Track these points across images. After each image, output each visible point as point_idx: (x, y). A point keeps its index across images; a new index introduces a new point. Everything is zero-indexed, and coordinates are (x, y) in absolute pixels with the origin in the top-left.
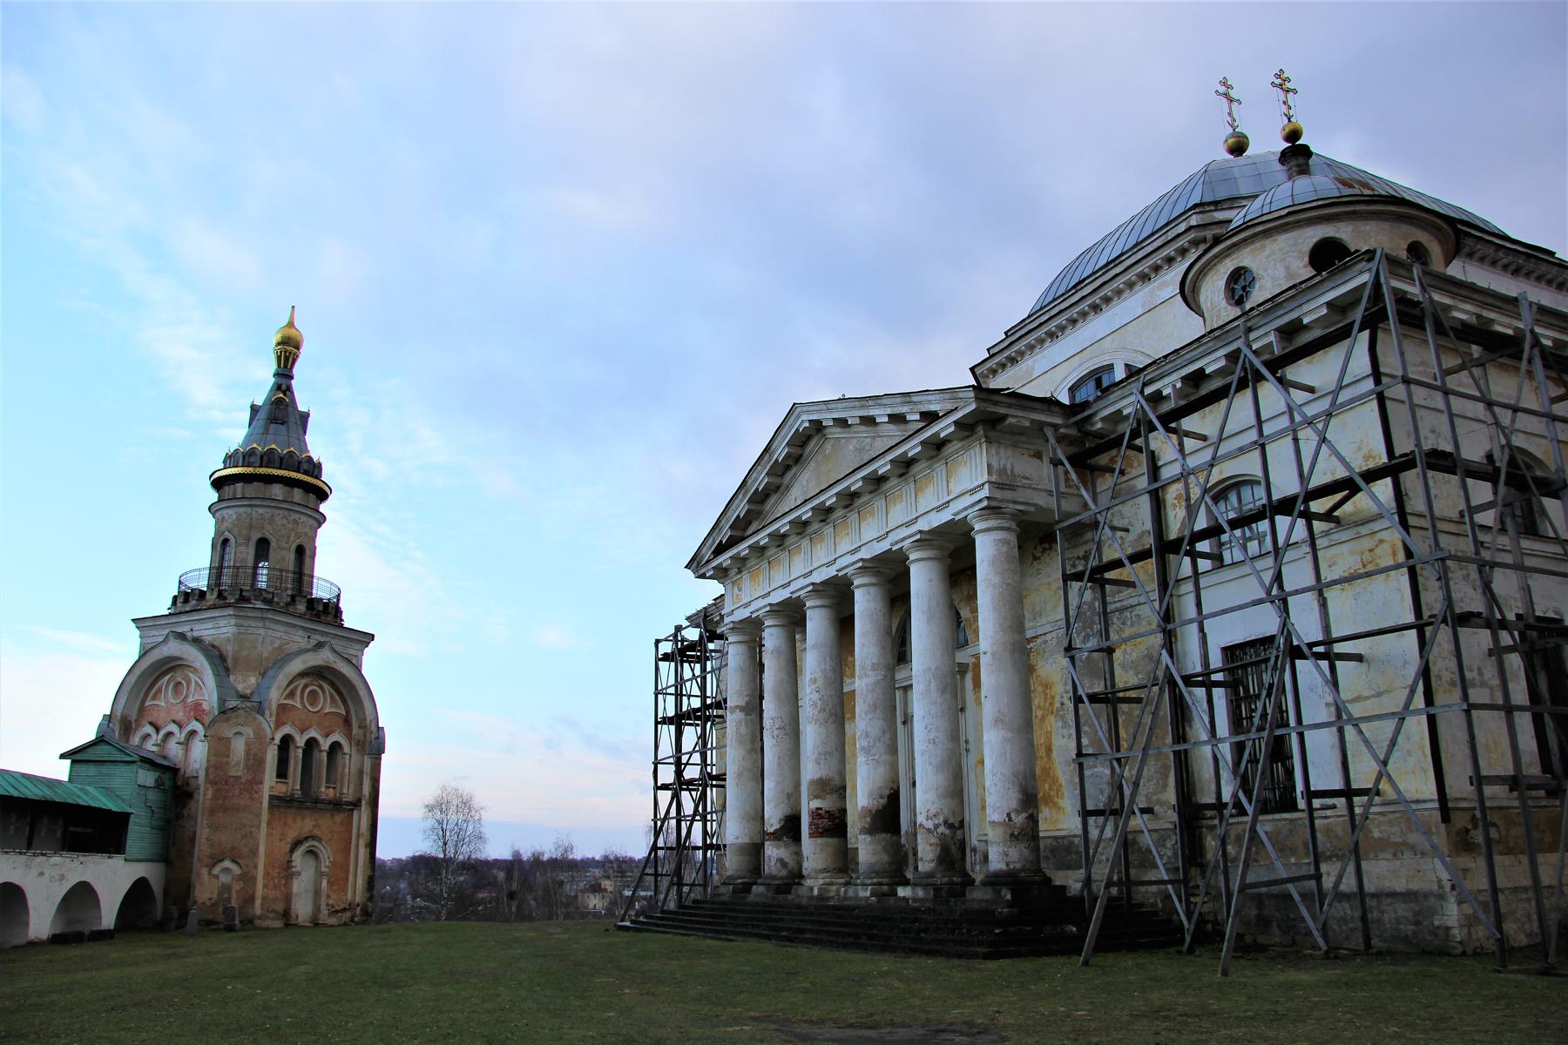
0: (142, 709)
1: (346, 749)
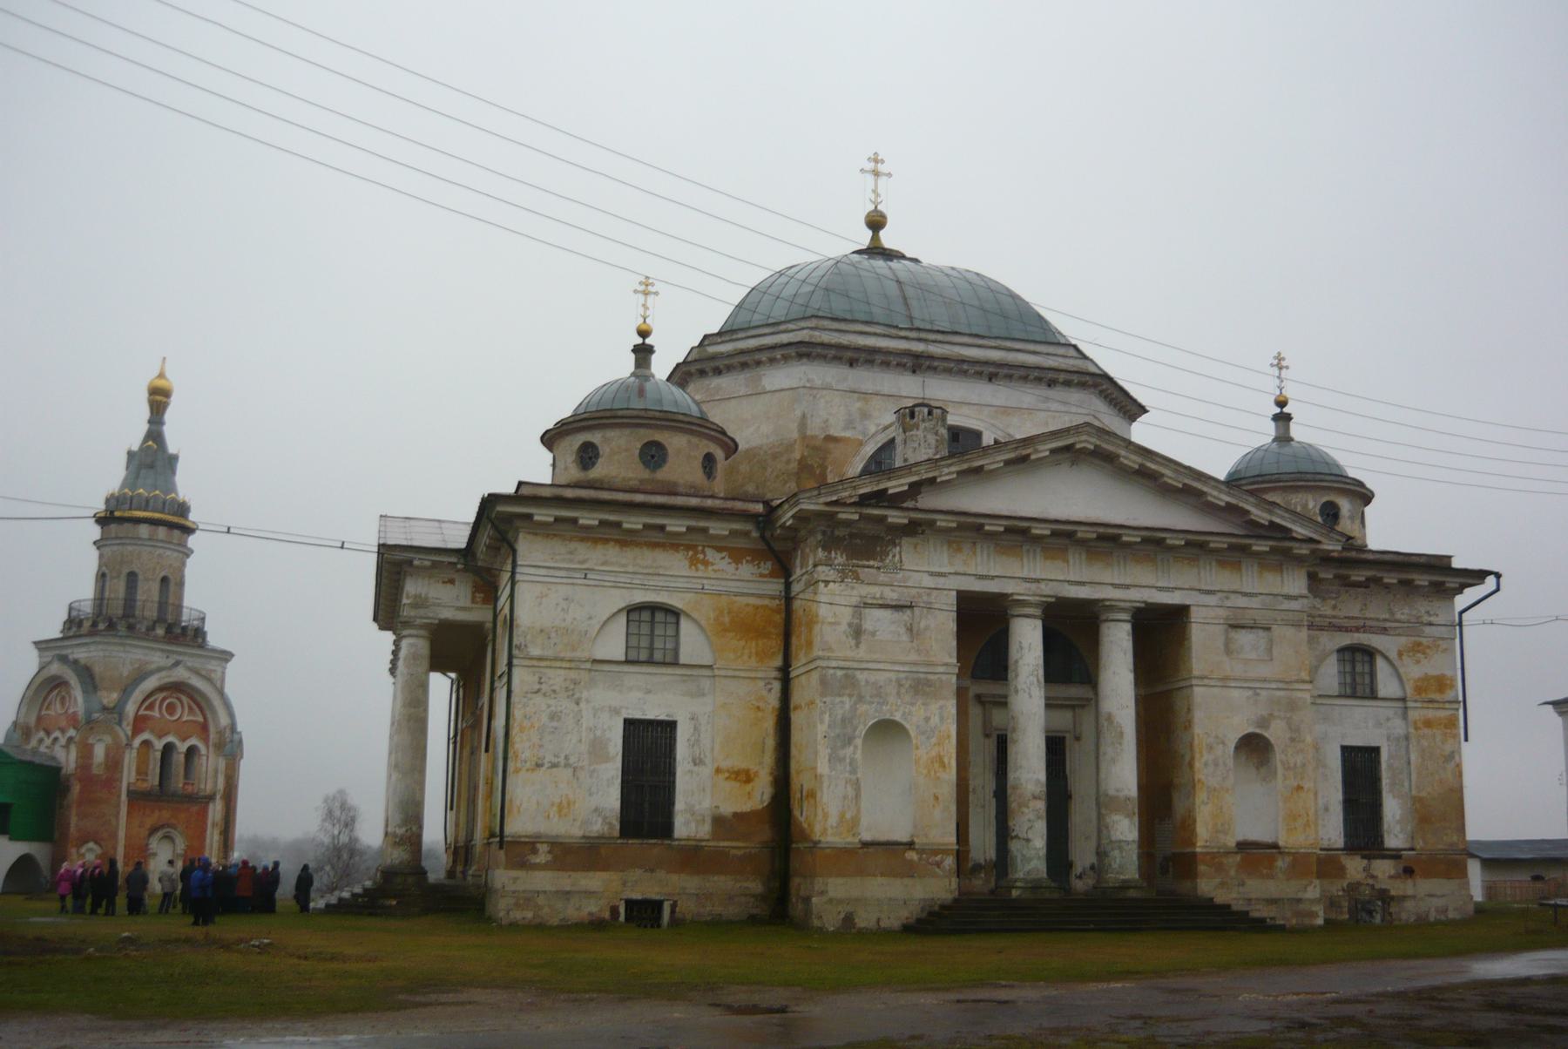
0: (39, 719)
1: (203, 750)
